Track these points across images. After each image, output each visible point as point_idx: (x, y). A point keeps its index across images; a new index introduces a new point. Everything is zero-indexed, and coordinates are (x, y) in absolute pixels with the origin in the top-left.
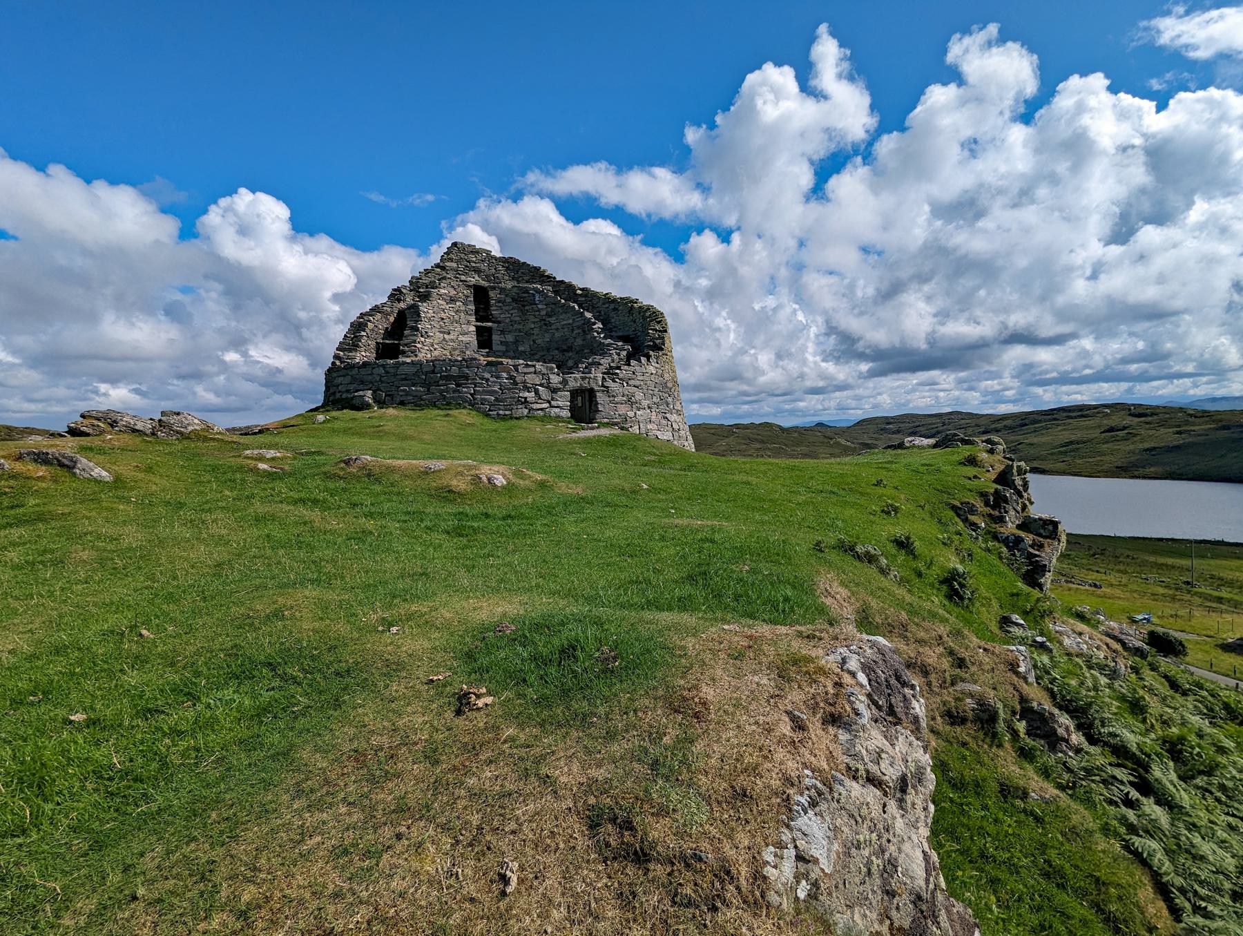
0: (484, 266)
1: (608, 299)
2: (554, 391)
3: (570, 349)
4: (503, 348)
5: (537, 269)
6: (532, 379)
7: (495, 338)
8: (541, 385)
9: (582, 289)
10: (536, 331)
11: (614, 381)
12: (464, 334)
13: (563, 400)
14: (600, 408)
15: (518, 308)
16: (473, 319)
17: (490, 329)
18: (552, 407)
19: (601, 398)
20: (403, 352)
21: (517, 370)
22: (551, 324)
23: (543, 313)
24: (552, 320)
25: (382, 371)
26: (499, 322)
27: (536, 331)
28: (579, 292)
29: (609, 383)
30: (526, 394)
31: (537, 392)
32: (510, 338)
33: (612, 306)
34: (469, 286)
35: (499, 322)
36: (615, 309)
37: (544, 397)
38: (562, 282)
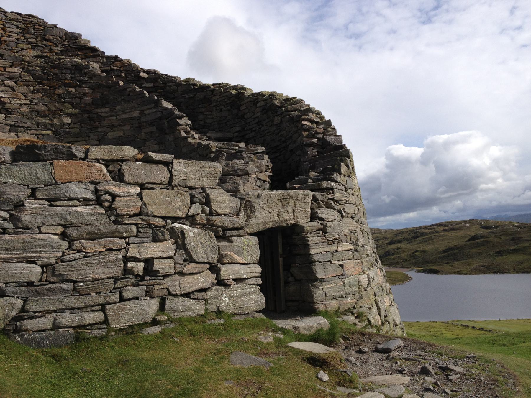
1: (190, 86)
2: (223, 234)
6: (165, 203)
8: (191, 220)
9: (148, 72)
11: (329, 206)
13: (245, 259)
14: (320, 272)
15: (45, 91)
19: (317, 248)
21: (119, 177)
22: (100, 118)
23: (89, 100)
24: (104, 111)
29: (323, 212)
30: (153, 250)
31: (180, 242)
33: (200, 95)
37: (199, 253)
38: (116, 58)
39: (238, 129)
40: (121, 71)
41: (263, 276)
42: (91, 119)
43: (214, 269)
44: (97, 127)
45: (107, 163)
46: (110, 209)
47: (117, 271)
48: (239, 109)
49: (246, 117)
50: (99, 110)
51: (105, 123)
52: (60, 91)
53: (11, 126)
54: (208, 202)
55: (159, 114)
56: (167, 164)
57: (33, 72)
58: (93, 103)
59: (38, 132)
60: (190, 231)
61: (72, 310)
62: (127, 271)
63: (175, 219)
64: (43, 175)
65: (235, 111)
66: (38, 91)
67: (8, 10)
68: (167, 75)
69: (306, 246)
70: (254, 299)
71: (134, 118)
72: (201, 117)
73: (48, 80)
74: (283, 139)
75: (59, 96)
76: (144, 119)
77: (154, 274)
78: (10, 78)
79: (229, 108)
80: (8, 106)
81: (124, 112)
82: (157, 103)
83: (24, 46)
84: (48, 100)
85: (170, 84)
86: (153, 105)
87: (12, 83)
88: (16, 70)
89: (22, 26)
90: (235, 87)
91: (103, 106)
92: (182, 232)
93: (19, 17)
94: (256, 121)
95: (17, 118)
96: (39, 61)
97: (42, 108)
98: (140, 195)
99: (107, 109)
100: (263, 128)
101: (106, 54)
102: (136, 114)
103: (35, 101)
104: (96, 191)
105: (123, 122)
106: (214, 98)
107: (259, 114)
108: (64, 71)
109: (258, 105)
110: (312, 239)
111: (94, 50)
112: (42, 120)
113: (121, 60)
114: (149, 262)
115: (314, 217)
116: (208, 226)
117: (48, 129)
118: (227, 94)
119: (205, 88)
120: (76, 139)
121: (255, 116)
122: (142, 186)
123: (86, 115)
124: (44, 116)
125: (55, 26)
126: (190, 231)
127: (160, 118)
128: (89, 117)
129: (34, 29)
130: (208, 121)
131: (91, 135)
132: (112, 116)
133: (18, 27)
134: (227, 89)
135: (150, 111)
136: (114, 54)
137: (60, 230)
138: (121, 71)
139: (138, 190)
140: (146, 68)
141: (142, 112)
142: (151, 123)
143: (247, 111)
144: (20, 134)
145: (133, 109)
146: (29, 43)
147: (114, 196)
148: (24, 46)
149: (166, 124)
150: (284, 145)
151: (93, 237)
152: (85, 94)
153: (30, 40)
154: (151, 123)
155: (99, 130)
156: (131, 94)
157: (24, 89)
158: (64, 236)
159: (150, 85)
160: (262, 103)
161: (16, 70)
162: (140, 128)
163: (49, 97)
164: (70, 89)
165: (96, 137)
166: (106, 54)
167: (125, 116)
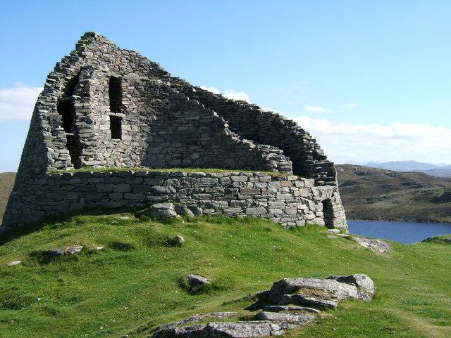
0: (112, 57)
6: (305, 193)
7: (125, 127)
8: (309, 198)
9: (196, 88)
16: (108, 108)
17: (121, 118)
20: (86, 146)
21: (294, 185)
24: (177, 115)
26: (128, 113)
30: (304, 207)
33: (229, 107)
34: (108, 77)
41: (324, 215)
43: (315, 213)
48: (255, 118)
52: (154, 101)
54: (312, 192)
55: (212, 120)
60: (310, 201)
62: (298, 212)
65: (252, 120)
66: (142, 101)
69: (332, 206)
70: (323, 223)
77: (304, 213)
80: (127, 110)
81: (189, 116)
82: (211, 114)
87: (130, 96)
90: (252, 106)
91: (176, 111)
101: (171, 76)
102: (197, 118)
110: (333, 203)
111: (166, 73)
112: (143, 117)
114: (302, 210)
115: (332, 196)
116: (313, 200)
117: (146, 123)
119: (231, 102)
122: (299, 188)
127: (212, 122)
133: (127, 59)
141: (201, 118)
142: (206, 125)
145: (195, 115)
151: (290, 202)
157: (135, 99)
162: (198, 126)
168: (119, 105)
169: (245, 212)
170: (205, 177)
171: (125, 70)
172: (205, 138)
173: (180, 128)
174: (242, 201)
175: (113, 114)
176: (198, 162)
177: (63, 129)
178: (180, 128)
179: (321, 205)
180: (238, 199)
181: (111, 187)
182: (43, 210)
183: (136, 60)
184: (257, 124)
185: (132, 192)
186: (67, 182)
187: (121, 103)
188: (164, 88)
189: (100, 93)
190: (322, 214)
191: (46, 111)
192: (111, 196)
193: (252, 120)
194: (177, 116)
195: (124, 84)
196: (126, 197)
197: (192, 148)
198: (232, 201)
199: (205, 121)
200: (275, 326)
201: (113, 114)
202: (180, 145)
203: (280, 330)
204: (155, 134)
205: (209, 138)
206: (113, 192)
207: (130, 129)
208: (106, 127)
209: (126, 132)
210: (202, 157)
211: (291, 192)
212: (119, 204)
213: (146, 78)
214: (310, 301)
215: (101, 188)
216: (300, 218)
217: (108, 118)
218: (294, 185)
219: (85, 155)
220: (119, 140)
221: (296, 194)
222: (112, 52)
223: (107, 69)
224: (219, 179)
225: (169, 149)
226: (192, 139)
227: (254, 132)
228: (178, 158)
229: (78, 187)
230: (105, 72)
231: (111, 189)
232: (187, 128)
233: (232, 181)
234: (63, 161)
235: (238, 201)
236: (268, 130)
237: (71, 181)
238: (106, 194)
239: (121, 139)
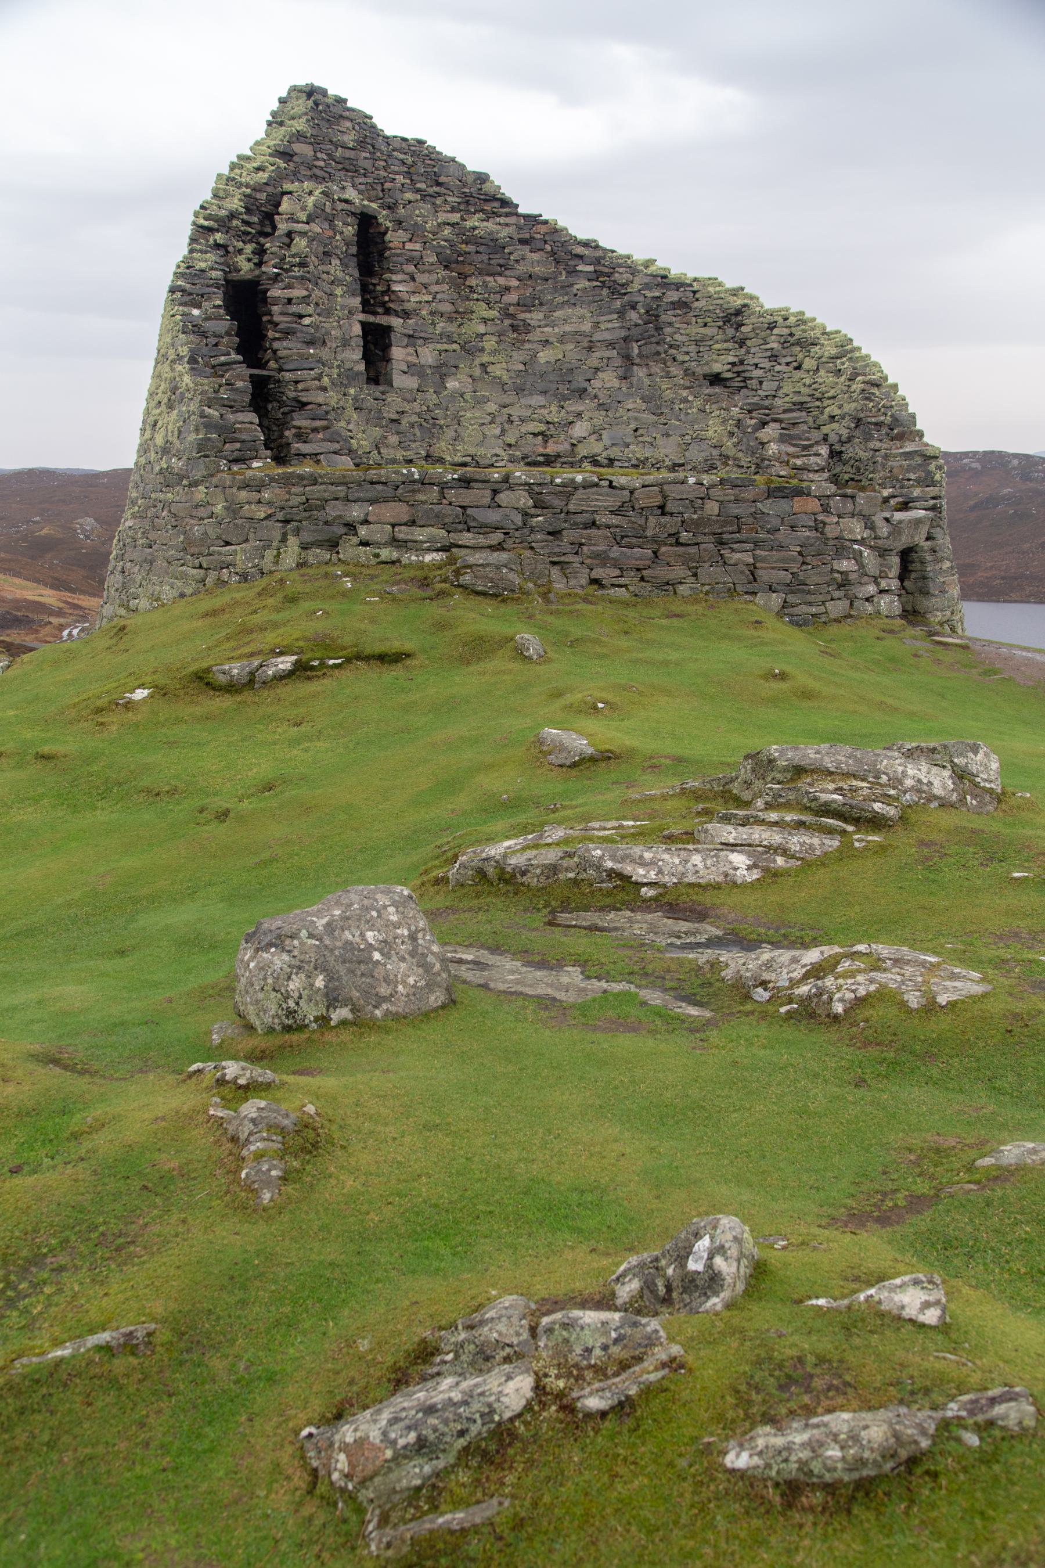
3: (582, 393)
4: (411, 382)
5: (482, 178)
7: (398, 353)
8: (862, 542)
9: (586, 244)
10: (490, 343)
12: (345, 343)
15: (452, 282)
16: (356, 302)
17: (389, 329)
18: (881, 592)
21: (826, 509)
22: (528, 328)
23: (512, 298)
24: (535, 317)
25: (525, 500)
26: (406, 315)
27: (490, 343)
28: (579, 250)
30: (845, 565)
31: (858, 557)
32: (428, 356)
33: (673, 296)
35: (406, 315)
36: (682, 305)
39: (731, 359)
40: (545, 242)
42: (514, 328)
44: (524, 341)
45: (819, 498)
46: (822, 533)
47: (828, 578)
49: (749, 343)
50: (528, 316)
51: (536, 336)
52: (473, 282)
53: (410, 336)
54: (872, 528)
55: (624, 333)
56: (853, 497)
57: (439, 250)
58: (518, 304)
59: (439, 347)
60: (866, 553)
61: (810, 604)
63: (855, 541)
64: (788, 509)
67: (388, 132)
68: (613, 251)
71: (582, 334)
72: (668, 330)
73: (457, 262)
74: (818, 395)
75: (472, 289)
76: (597, 337)
78: (409, 261)
79: (721, 324)
80: (408, 306)
83: (409, 196)
84: (456, 296)
85: (621, 270)
86: (616, 316)
88: (418, 246)
89: (410, 160)
90: (736, 292)
92: (861, 552)
93: (404, 145)
94: (769, 354)
95: (416, 324)
96: (447, 231)
97: (446, 307)
98: (838, 523)
99: (541, 316)
100: (778, 368)
101: (520, 210)
102: (586, 327)
103: (439, 296)
104: (816, 520)
105: (562, 339)
106: (696, 304)
107: (775, 345)
108: (481, 249)
109: (776, 331)
110: (928, 557)
111: (505, 202)
113: (546, 222)
118: (720, 302)
120: (492, 359)
121: (768, 346)
122: (839, 517)
123: (507, 322)
124: (450, 320)
125: (453, 160)
126: (866, 553)
127: (625, 339)
128: (512, 326)
129: (426, 166)
130: (677, 337)
131: (514, 354)
132: (546, 326)
134: (718, 292)
135: (610, 325)
136: (534, 211)
137: (798, 549)
138: (545, 242)
139: (835, 520)
140: (582, 236)
142: (611, 345)
143: (752, 335)
144: (419, 349)
146: (418, 191)
147: (825, 524)
148: (409, 196)
149: (636, 351)
150: (818, 403)
152: (508, 289)
153: (419, 185)
154: (611, 345)
155: (527, 346)
156: (580, 294)
157: (422, 278)
158: (800, 553)
159: (591, 268)
160: (786, 331)
161: (418, 246)
162: (590, 349)
163: (458, 286)
164: (490, 279)
165: (521, 359)
166: (520, 210)
167: (568, 328)
168: (384, 293)
169: (695, 575)
170: (597, 485)
171: (398, 195)
172: (609, 379)
173: (545, 356)
174: (693, 550)
175: (371, 319)
176: (582, 451)
177: (240, 358)
178: (545, 356)
179: (895, 560)
180: (678, 544)
181: (356, 512)
182: (201, 567)
183: (423, 165)
184: (742, 344)
185: (413, 523)
186: (255, 496)
187: (388, 291)
188: (495, 246)
189: (335, 262)
190: (894, 584)
191: (196, 312)
192: (363, 531)
193: (730, 332)
194: (532, 323)
195: (395, 238)
196: (401, 536)
197: (573, 406)
198: (663, 549)
199: (607, 336)
200: (740, 860)
201: (371, 319)
202: (538, 400)
203: (749, 868)
204: (477, 372)
205: (616, 383)
206: (366, 522)
207: (413, 359)
208: (354, 356)
209: (405, 369)
210: (597, 432)
211: (819, 527)
212: (385, 553)
213: (455, 217)
214: (826, 804)
215: (332, 511)
216: (836, 594)
217: (357, 329)
218: (826, 509)
219: (295, 427)
220: (387, 388)
221: (831, 532)
222: (362, 143)
223: (351, 194)
224: (632, 492)
225: (515, 412)
226: (574, 385)
227: (733, 364)
228: (535, 435)
229: (282, 508)
230: (346, 201)
231: (362, 517)
232: (560, 357)
233: (665, 497)
234: (243, 441)
235: (680, 550)
236: (774, 357)
237: (266, 495)
238: (351, 527)
239: (390, 384)
